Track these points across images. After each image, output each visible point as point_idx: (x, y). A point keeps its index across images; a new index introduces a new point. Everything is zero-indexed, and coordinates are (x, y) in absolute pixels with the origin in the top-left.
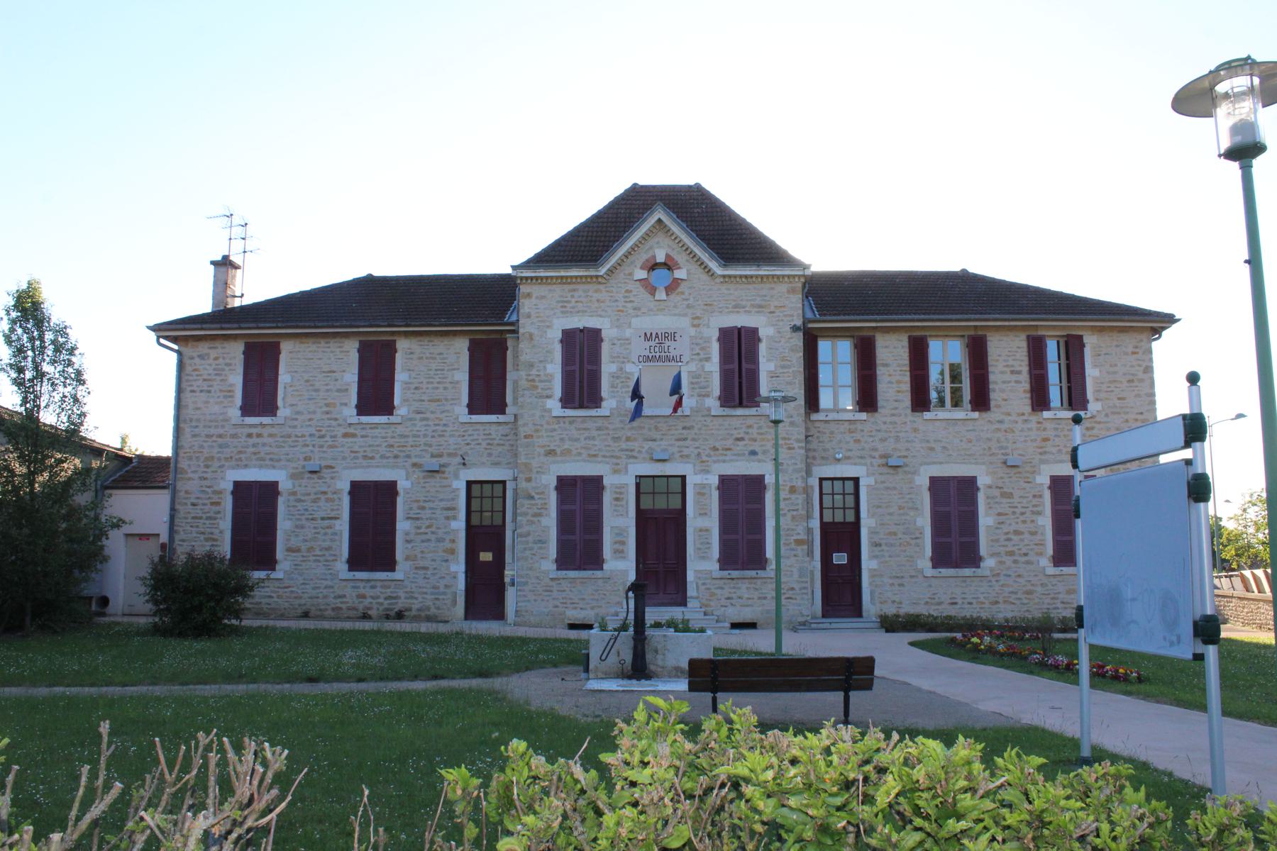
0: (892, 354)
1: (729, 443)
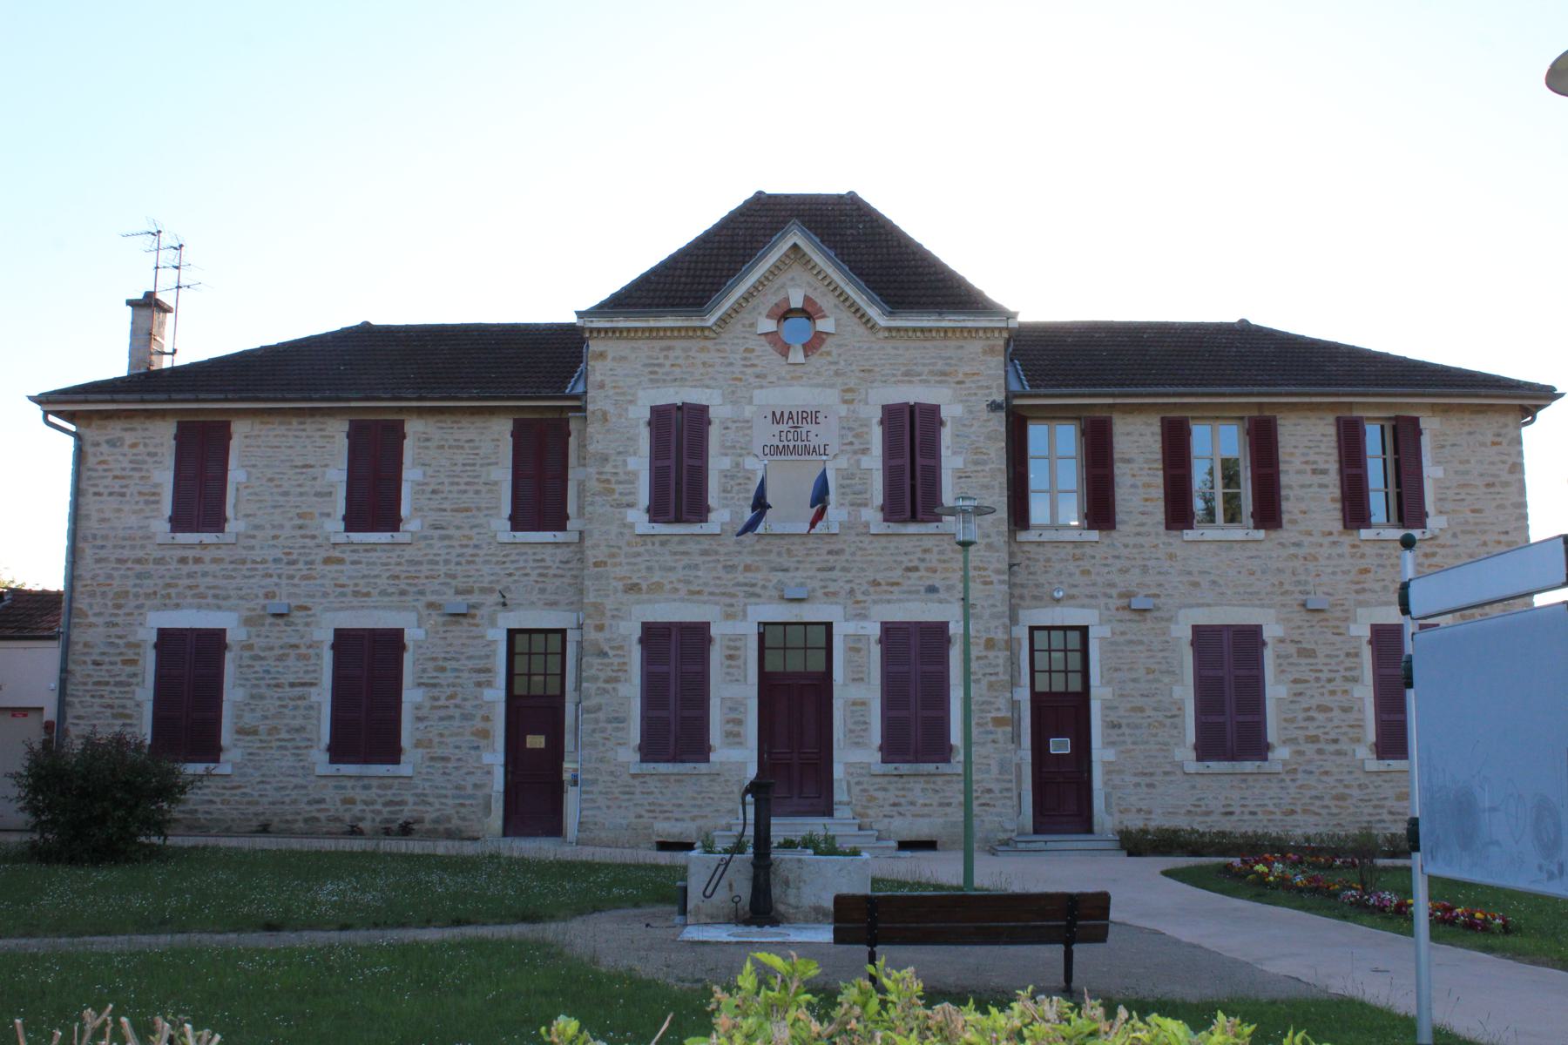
0: (1137, 445)
1: (896, 574)
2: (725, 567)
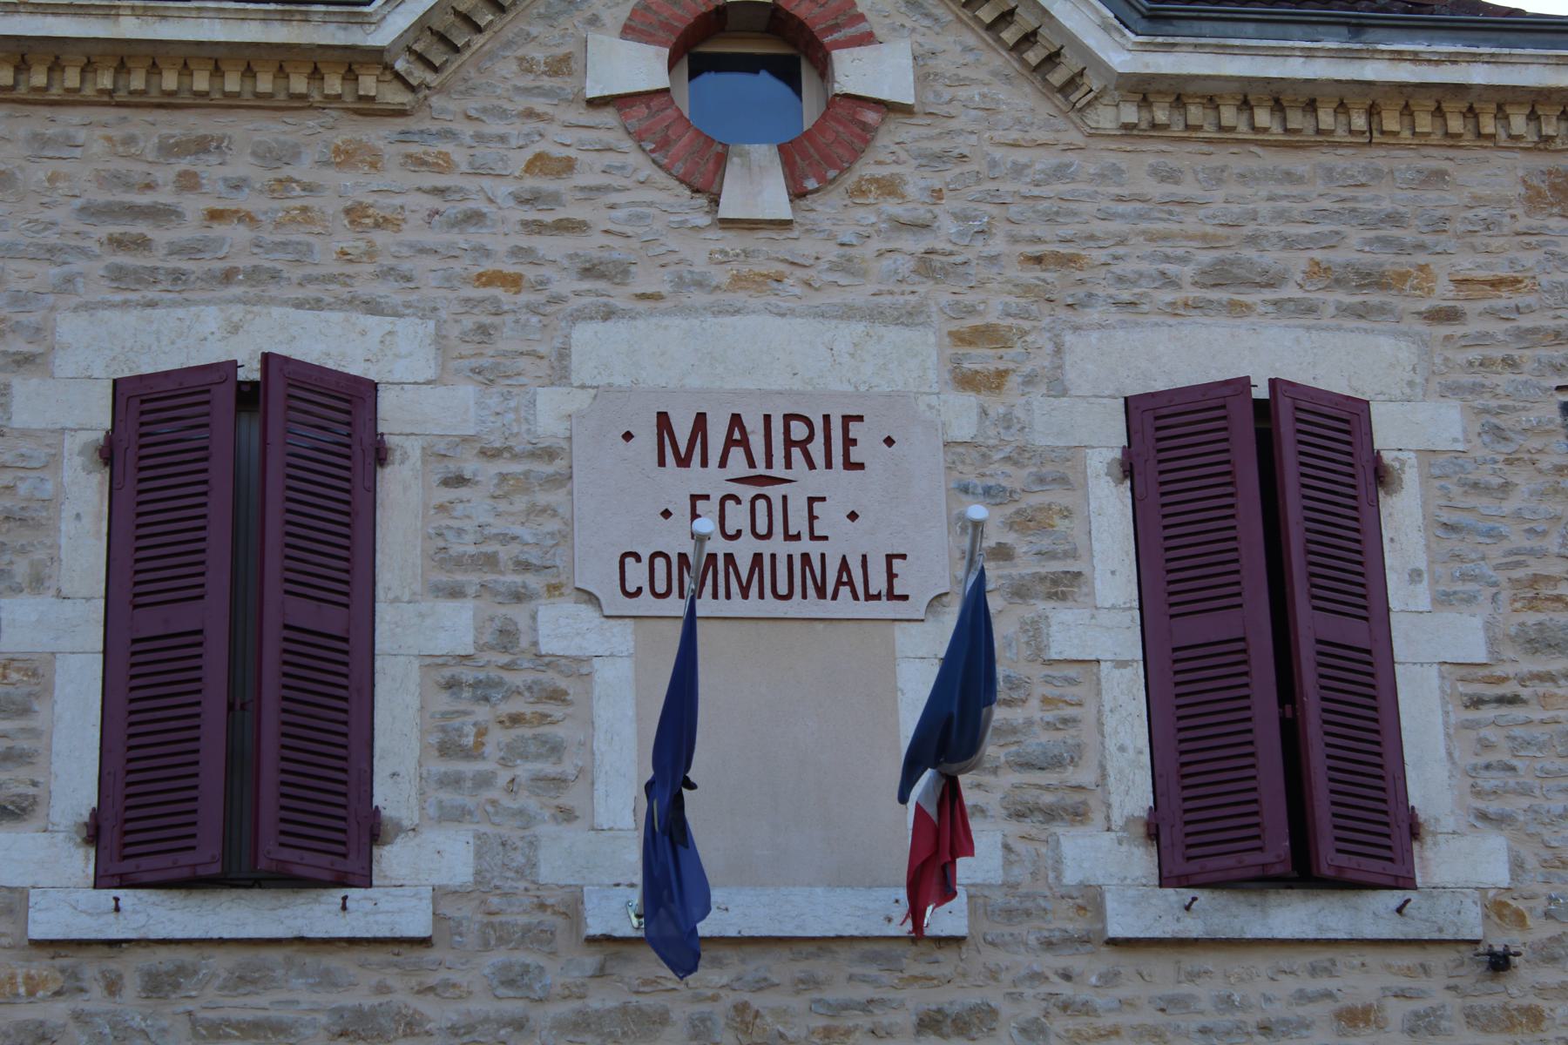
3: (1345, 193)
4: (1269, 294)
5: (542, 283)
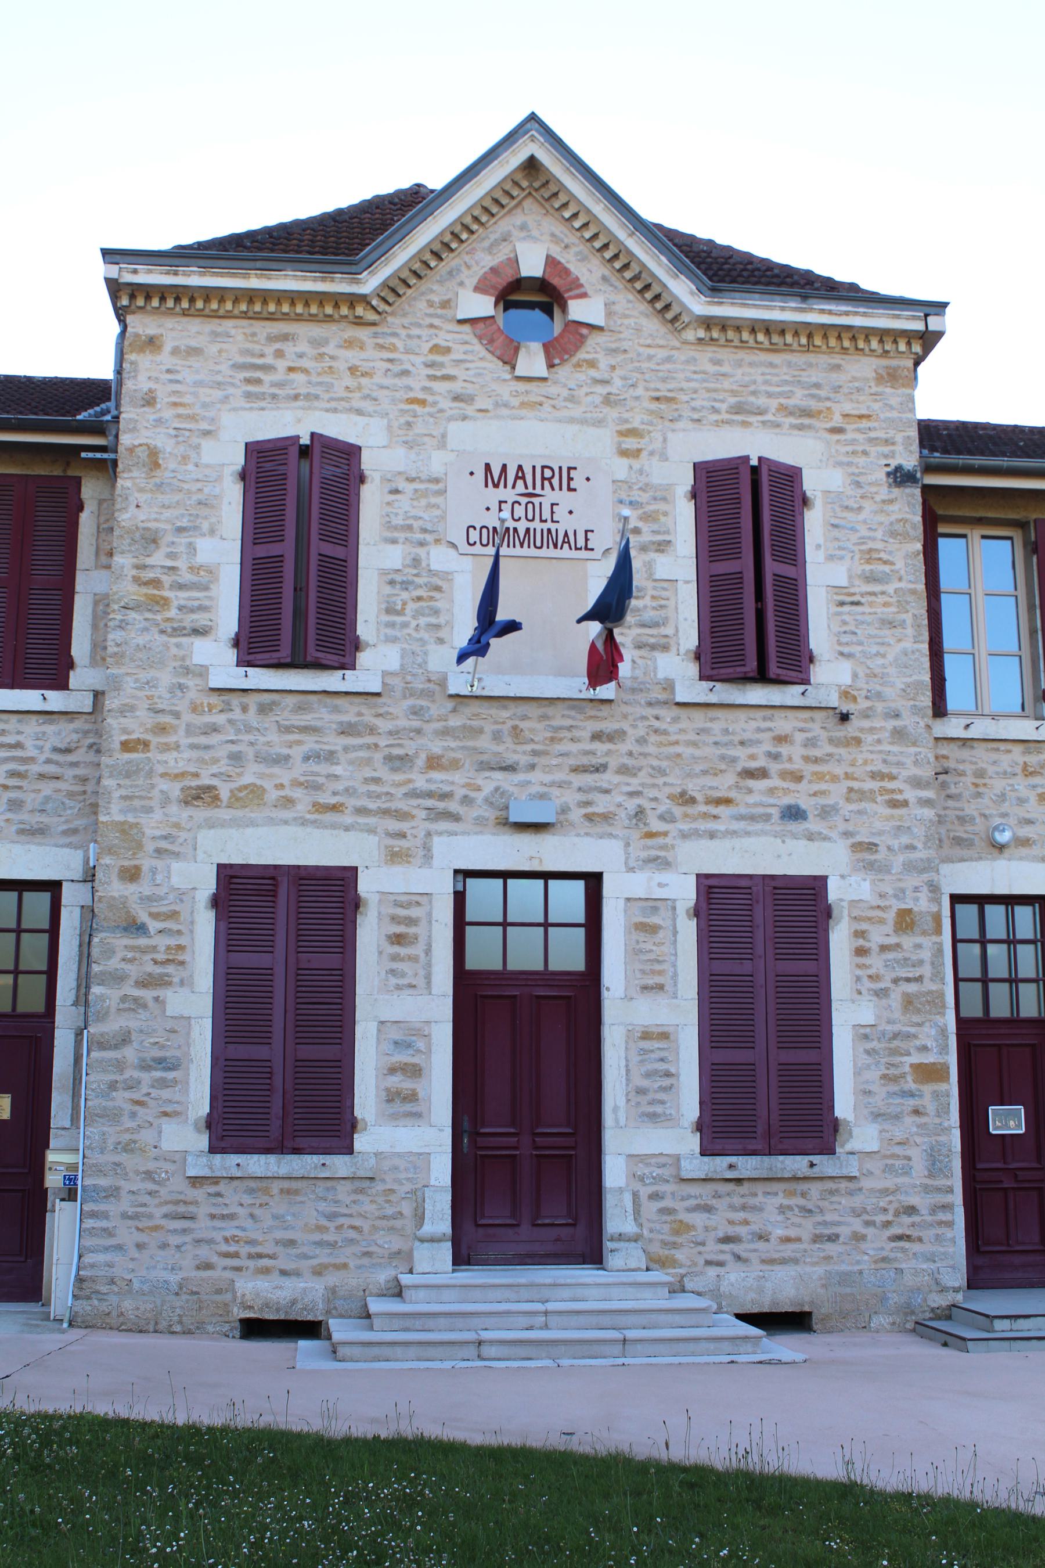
1: (725, 783)
2: (389, 758)
3: (796, 373)
4: (760, 418)
5: (435, 403)
